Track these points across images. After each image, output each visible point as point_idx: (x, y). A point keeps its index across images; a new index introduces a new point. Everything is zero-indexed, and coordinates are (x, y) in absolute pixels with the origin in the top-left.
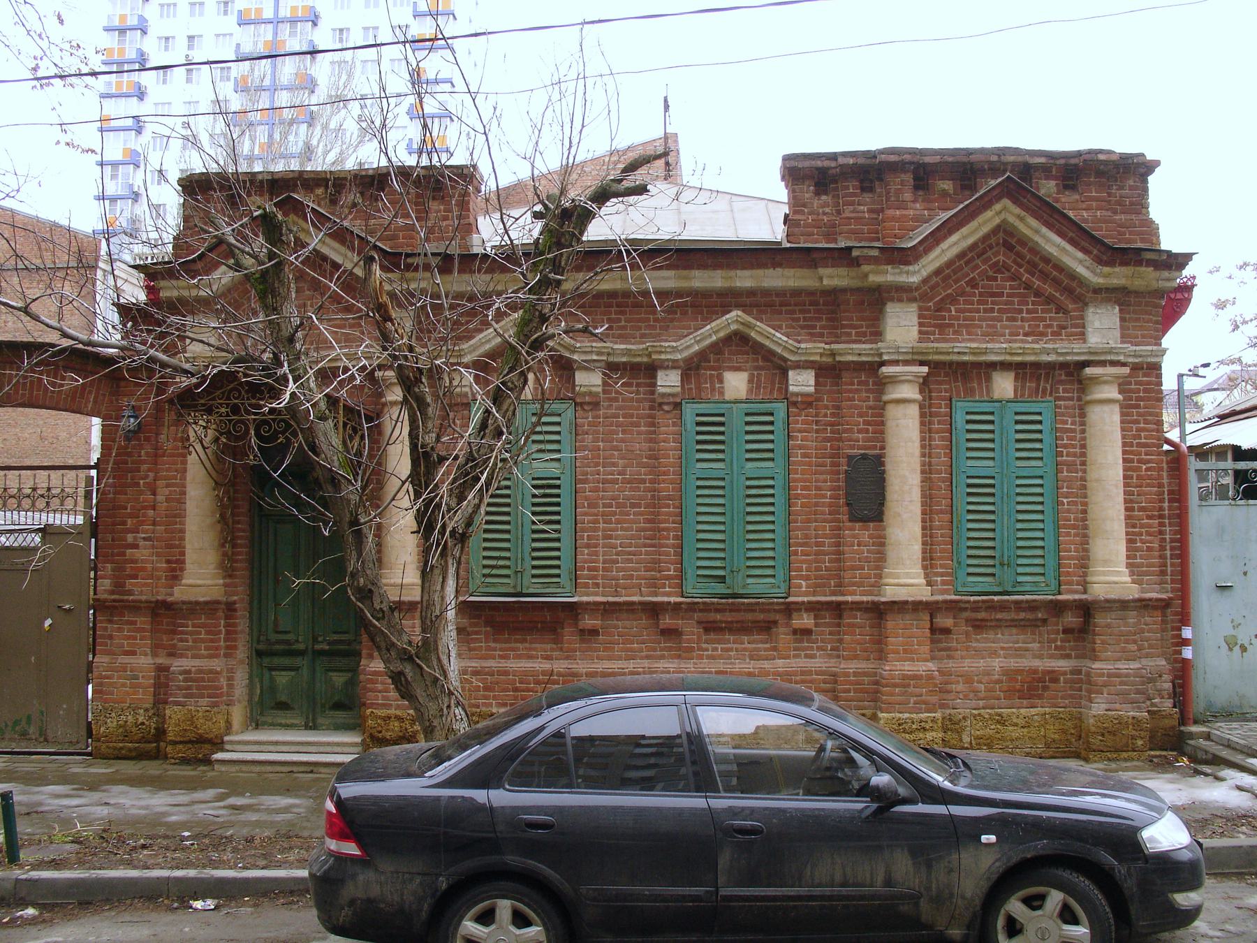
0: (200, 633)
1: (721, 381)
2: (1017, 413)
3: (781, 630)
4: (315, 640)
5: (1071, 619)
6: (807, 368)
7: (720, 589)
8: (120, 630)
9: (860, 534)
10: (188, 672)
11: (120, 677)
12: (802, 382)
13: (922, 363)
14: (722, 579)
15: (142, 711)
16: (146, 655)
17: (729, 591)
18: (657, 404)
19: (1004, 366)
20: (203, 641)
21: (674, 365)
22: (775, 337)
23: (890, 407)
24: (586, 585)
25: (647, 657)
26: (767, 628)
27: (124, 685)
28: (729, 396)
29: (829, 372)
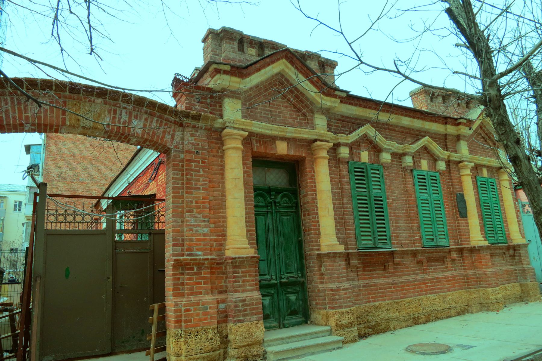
0: (246, 276)
1: (420, 163)
2: (355, 168)
3: (448, 259)
4: (281, 278)
5: (511, 252)
6: (346, 146)
7: (433, 244)
8: (190, 279)
9: (462, 222)
10: (245, 300)
11: (195, 310)
12: (442, 166)
13: (244, 130)
14: (433, 240)
15: (210, 331)
16: (208, 294)
17: (436, 244)
18: (404, 169)
19: (283, 139)
20: (248, 281)
21: (345, 145)
22: (380, 139)
23: (462, 177)
24: (394, 243)
25: (414, 274)
26: (442, 260)
27: (198, 315)
28: (423, 169)
29: (448, 163)
